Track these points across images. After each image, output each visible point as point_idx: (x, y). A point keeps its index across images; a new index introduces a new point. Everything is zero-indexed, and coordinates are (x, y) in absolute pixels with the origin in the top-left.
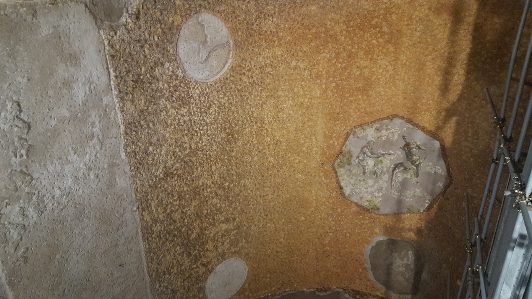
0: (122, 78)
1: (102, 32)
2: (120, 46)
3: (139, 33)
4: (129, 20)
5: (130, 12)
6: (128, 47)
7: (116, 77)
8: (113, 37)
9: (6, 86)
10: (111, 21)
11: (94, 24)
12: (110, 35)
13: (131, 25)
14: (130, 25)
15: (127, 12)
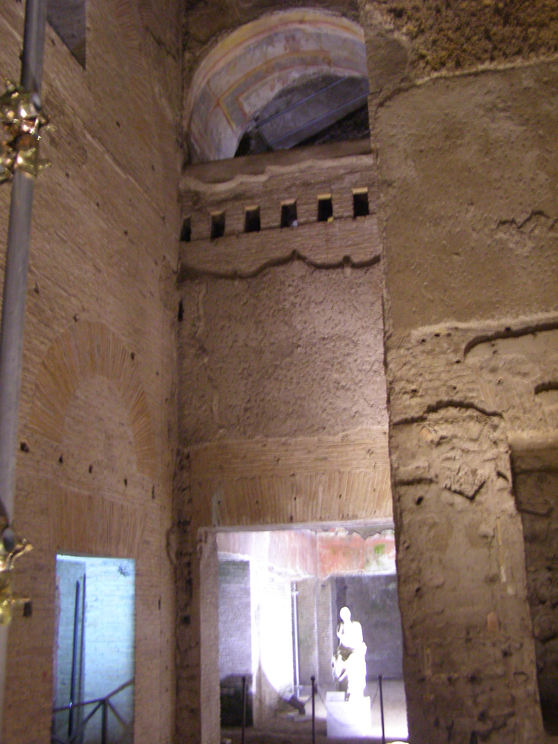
0: (495, 48)
1: (419, 82)
2: (443, 49)
3: (424, 10)
4: (404, 30)
5: (392, 27)
6: (446, 32)
7: (492, 59)
8: (427, 63)
9: (475, 235)
10: (404, 62)
11: (406, 94)
12: (424, 68)
13: (411, 26)
14: (411, 28)
15: (392, 31)
